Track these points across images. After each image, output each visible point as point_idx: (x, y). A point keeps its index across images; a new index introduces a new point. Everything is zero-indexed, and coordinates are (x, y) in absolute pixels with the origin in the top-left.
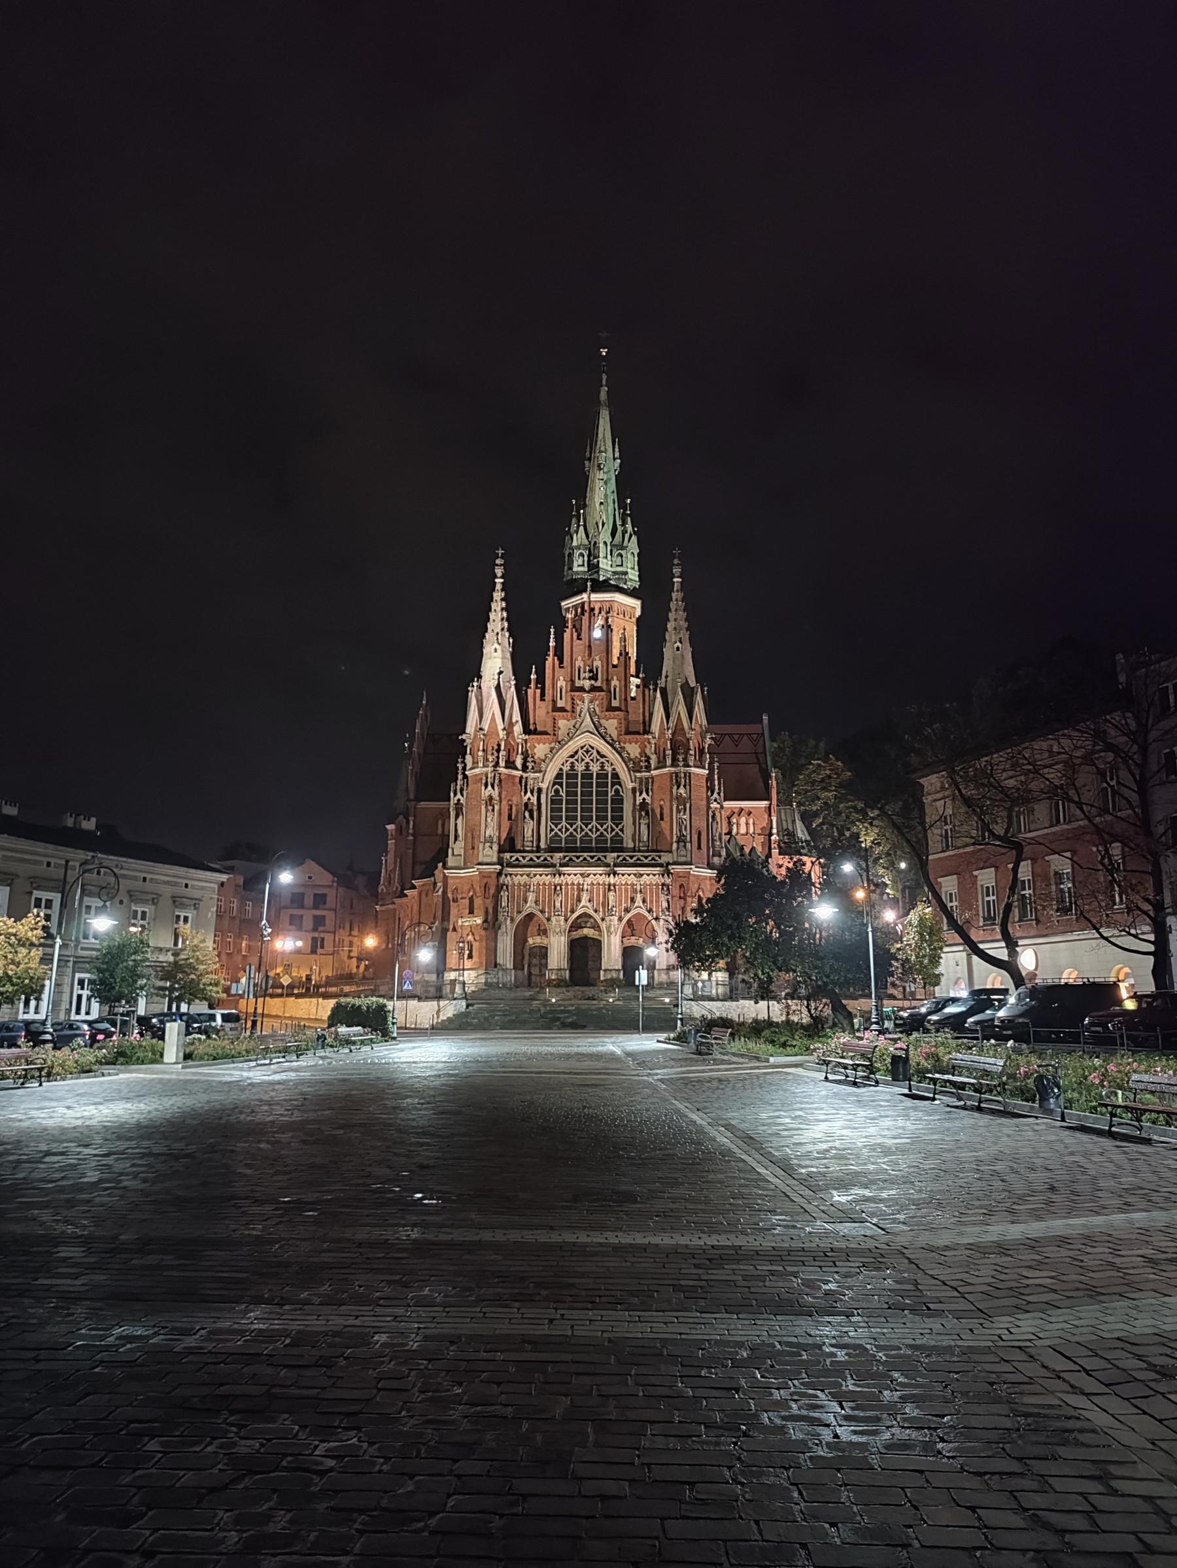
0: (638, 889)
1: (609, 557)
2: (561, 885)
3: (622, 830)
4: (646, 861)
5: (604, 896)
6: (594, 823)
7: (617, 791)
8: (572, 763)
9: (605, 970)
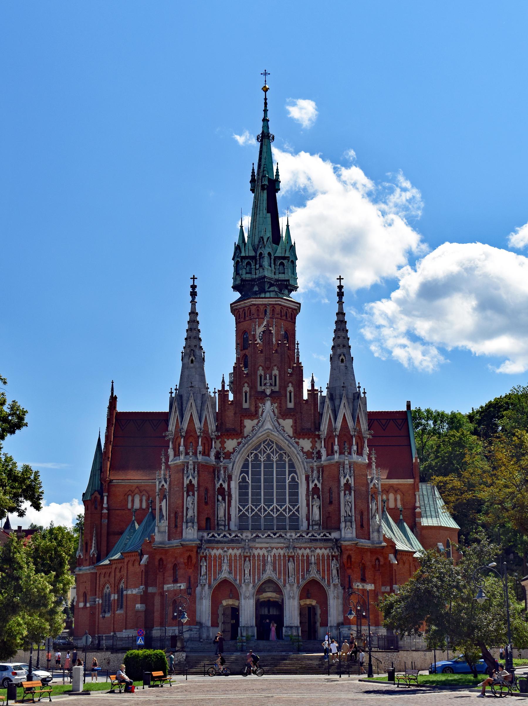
1: (273, 265)
2: (249, 557)
3: (297, 510)
4: (319, 537)
5: (285, 565)
6: (275, 504)
7: (293, 478)
8: (256, 455)
9: (287, 627)
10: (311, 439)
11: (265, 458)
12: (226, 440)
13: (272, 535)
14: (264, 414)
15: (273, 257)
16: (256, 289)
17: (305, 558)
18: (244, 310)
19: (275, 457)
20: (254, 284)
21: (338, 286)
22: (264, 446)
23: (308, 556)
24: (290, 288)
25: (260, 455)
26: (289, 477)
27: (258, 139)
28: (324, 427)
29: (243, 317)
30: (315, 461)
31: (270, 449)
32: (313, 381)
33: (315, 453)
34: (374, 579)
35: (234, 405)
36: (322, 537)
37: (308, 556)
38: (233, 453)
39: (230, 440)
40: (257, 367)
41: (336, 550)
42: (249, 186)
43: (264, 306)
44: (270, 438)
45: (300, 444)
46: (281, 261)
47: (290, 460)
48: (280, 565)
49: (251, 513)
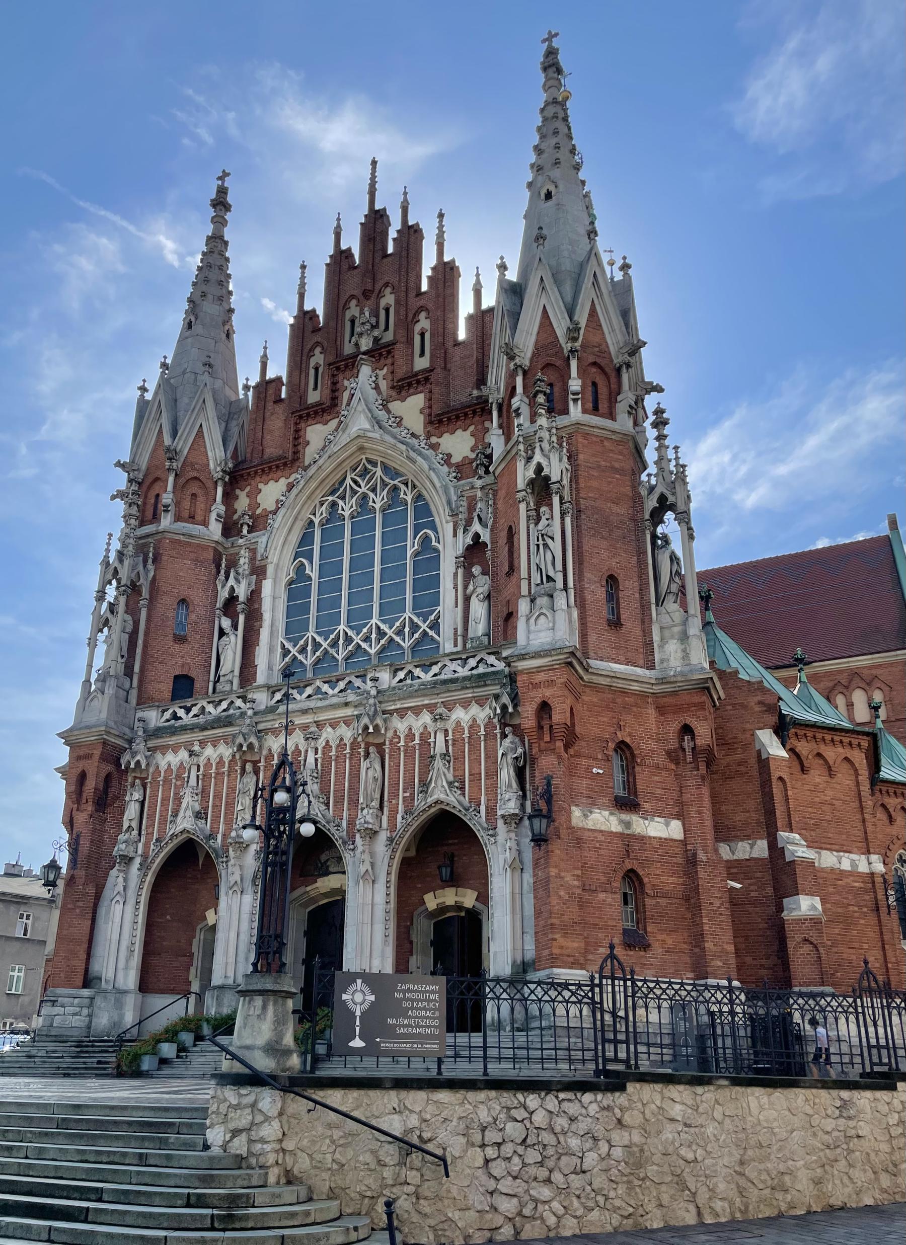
0: (440, 747)
10: (472, 428)
11: (354, 508)
12: (261, 486)
17: (417, 741)
22: (355, 482)
23: (425, 736)
25: (341, 503)
31: (368, 483)
34: (680, 803)
37: (425, 736)
38: (275, 513)
39: (272, 483)
40: (342, 302)
44: (369, 456)
47: (419, 497)
48: (340, 775)
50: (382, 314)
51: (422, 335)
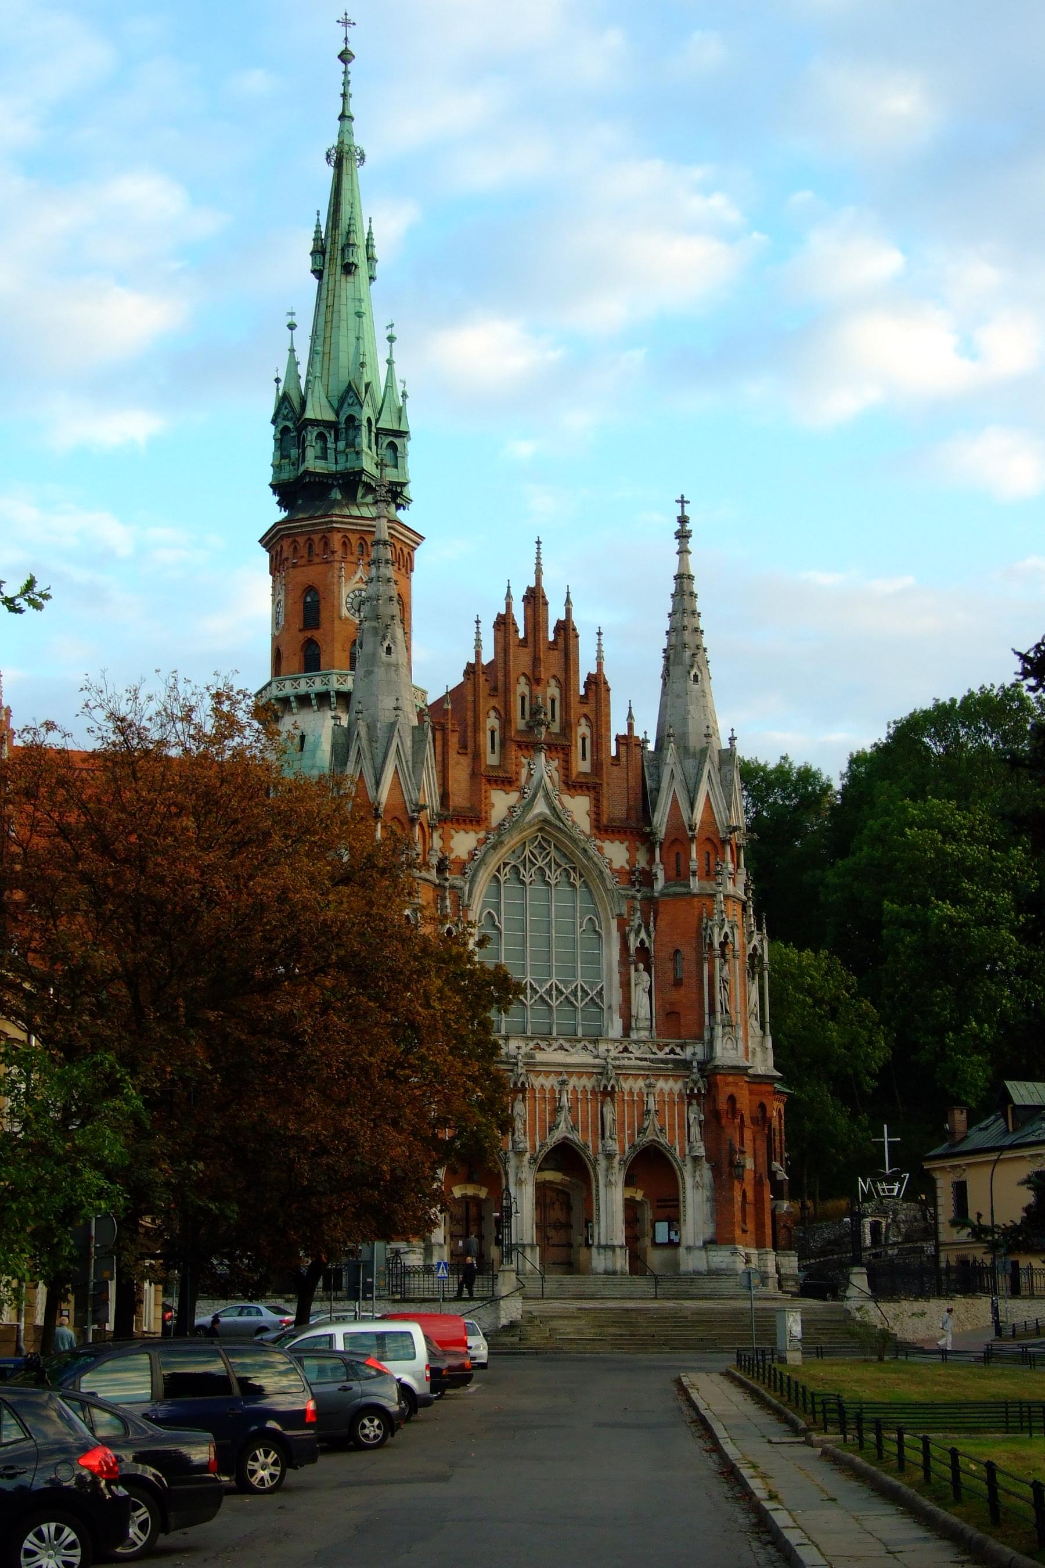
0: (652, 1106)
1: (374, 447)
3: (600, 993)
4: (661, 1055)
10: (626, 843)
12: (453, 832)
13: (567, 1045)
14: (535, 779)
15: (374, 429)
16: (336, 494)
17: (636, 1098)
18: (309, 539)
19: (553, 877)
20: (332, 483)
21: (679, 518)
22: (530, 851)
23: (640, 1094)
24: (399, 501)
26: (581, 923)
27: (328, 156)
28: (661, 819)
29: (306, 555)
30: (638, 891)
31: (544, 858)
32: (630, 716)
33: (637, 874)
35: (471, 756)
36: (667, 1054)
39: (462, 833)
41: (700, 1084)
42: (308, 262)
43: (358, 536)
45: (605, 851)
46: (391, 439)
49: (582, 1000)
50: (549, 702)
51: (584, 739)
